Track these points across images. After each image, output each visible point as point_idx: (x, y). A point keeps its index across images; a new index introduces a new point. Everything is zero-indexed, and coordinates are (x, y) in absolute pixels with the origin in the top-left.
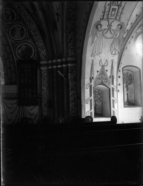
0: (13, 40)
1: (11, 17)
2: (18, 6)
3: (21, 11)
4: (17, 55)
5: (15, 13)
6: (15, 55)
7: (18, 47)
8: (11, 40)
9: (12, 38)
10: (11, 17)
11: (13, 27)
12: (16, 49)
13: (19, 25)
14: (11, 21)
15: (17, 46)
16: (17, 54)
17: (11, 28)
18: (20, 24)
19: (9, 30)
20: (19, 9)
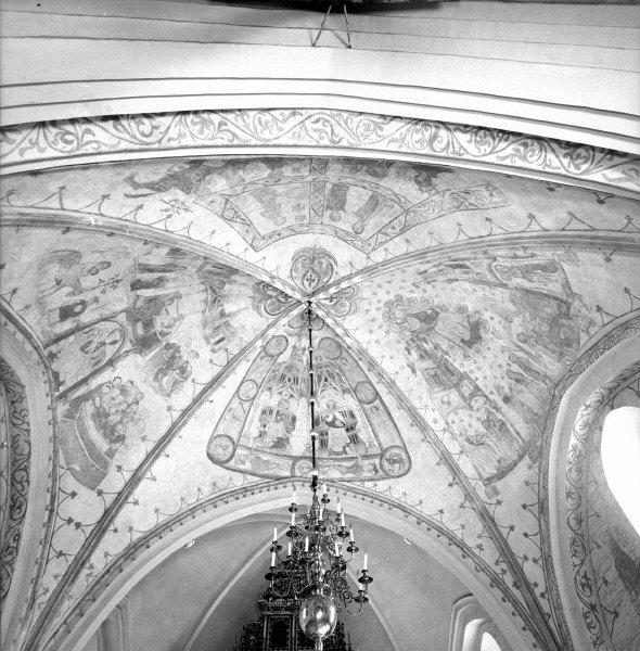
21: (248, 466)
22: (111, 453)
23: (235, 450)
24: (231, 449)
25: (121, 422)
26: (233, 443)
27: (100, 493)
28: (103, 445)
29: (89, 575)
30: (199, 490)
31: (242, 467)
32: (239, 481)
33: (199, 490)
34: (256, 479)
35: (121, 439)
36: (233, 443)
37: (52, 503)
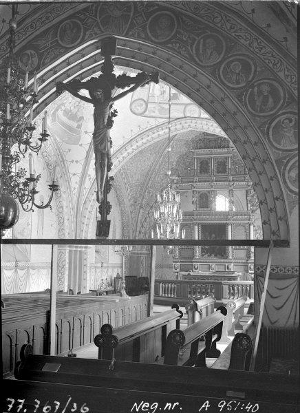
0: (279, 149)
1: (271, 100)
2: (286, 73)
3: (293, 83)
4: (289, 184)
5: (281, 89)
6: (285, 182)
7: (290, 165)
8: (274, 150)
9: (276, 145)
10: (271, 100)
11: (276, 121)
12: (285, 169)
13: (289, 115)
14: (274, 108)
15: (288, 162)
16: (287, 180)
17: (273, 124)
18: (291, 113)
19: (268, 129)
20: (289, 80)
21: (157, 114)
22: (79, 127)
23: (147, 106)
24: (144, 106)
25: (78, 111)
26: (145, 101)
27: (81, 145)
28: (75, 125)
29: (90, 179)
30: (132, 131)
31: (154, 114)
32: (153, 123)
33: (132, 131)
34: (163, 120)
35: (82, 118)
36: (145, 101)
37: (62, 158)
